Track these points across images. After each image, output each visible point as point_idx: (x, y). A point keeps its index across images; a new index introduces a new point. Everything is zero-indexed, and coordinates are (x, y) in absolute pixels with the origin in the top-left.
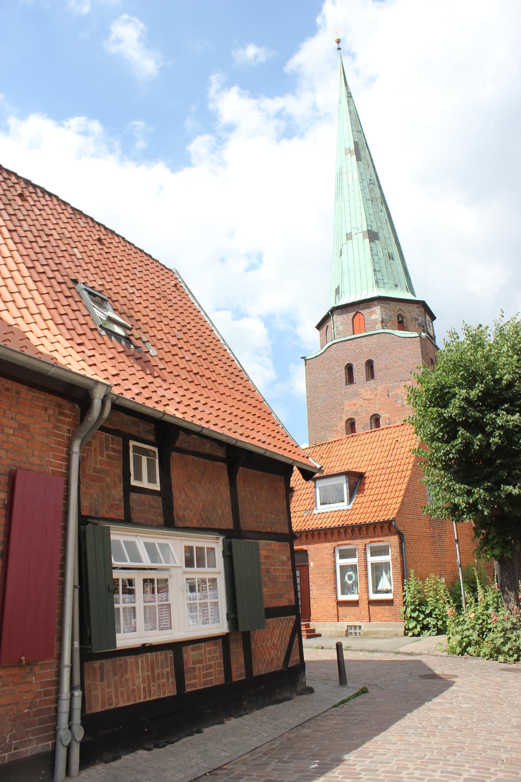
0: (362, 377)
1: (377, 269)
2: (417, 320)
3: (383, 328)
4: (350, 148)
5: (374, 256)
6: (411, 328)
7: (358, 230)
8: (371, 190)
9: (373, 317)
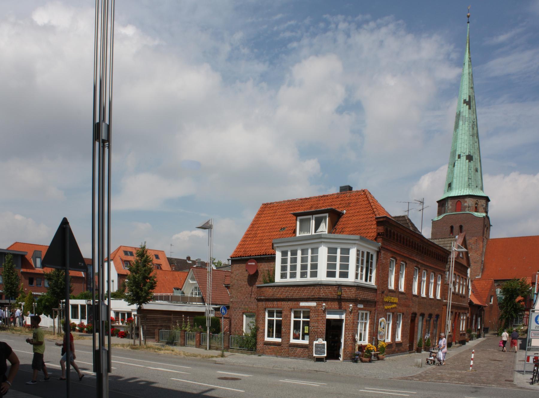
2: (483, 206)
6: (480, 210)
8: (473, 129)
9: (466, 204)
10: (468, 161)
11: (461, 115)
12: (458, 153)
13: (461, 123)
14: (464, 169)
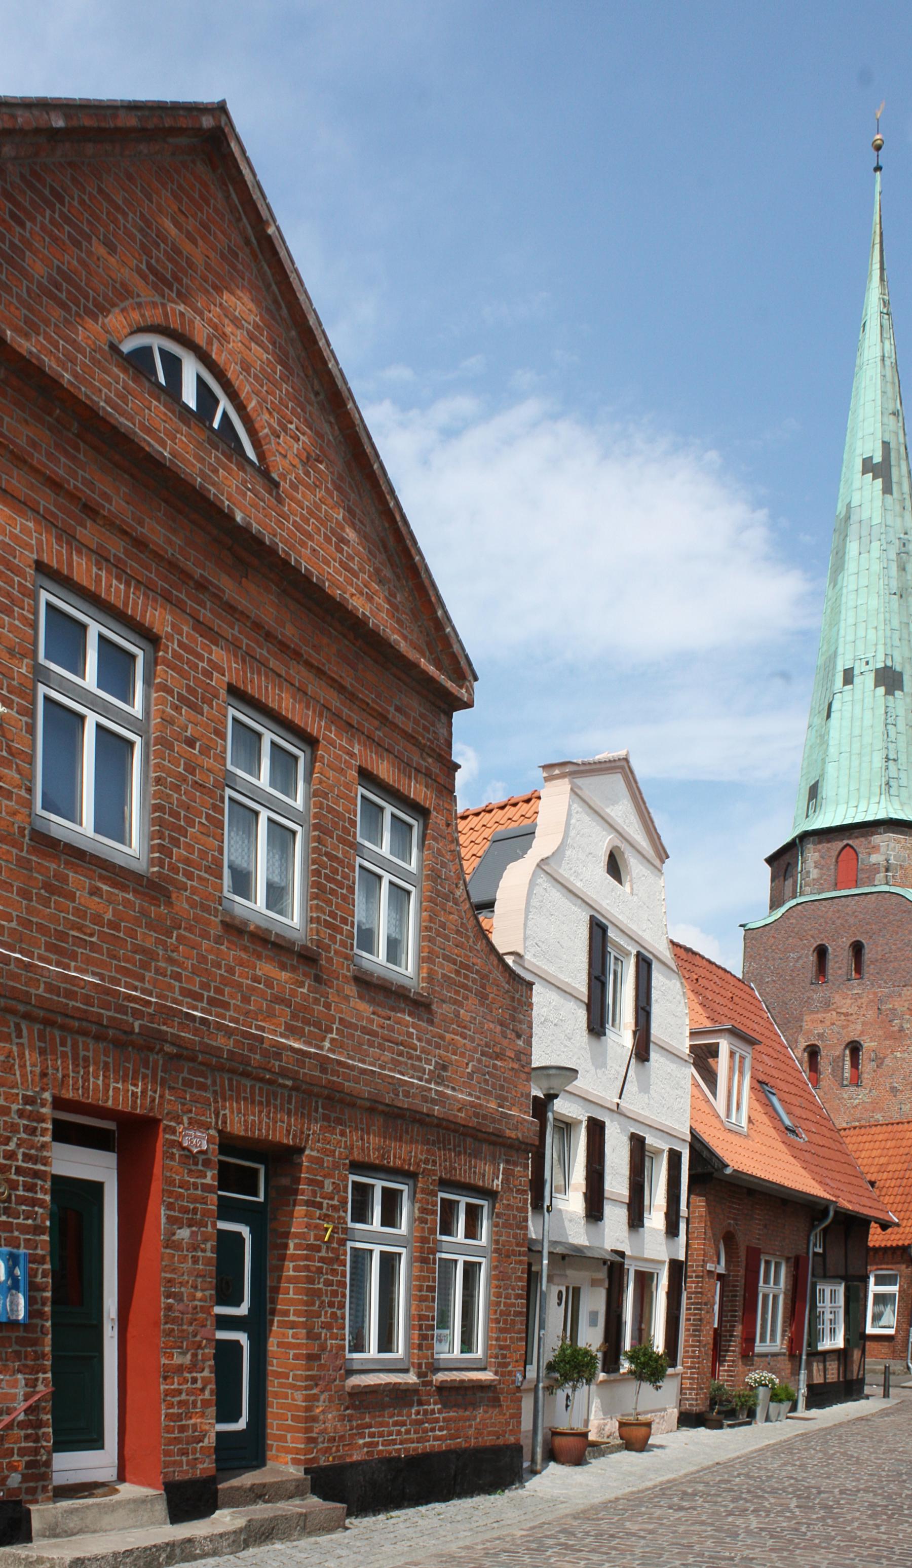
0: (840, 972)
1: (891, 757)
3: (887, 884)
4: (871, 458)
5: (889, 727)
7: (867, 663)
10: (881, 690)
11: (854, 518)
12: (841, 665)
13: (853, 548)
14: (867, 722)
